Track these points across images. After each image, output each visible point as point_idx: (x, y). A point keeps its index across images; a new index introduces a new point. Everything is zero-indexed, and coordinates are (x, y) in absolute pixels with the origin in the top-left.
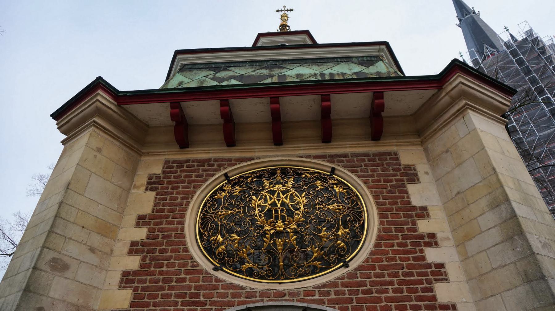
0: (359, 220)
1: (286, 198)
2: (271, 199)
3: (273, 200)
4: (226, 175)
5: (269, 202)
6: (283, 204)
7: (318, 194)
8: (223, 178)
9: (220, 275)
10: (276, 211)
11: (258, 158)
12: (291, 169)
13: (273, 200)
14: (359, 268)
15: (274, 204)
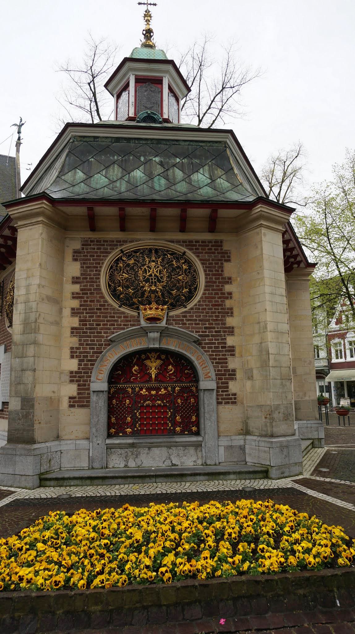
0: (194, 285)
1: (157, 272)
2: (149, 271)
3: (150, 273)
4: (121, 250)
5: (148, 274)
6: (155, 275)
7: (174, 269)
8: (120, 252)
9: (122, 309)
10: (152, 279)
11: (140, 240)
12: (160, 249)
13: (150, 273)
14: (192, 309)
15: (151, 275)
